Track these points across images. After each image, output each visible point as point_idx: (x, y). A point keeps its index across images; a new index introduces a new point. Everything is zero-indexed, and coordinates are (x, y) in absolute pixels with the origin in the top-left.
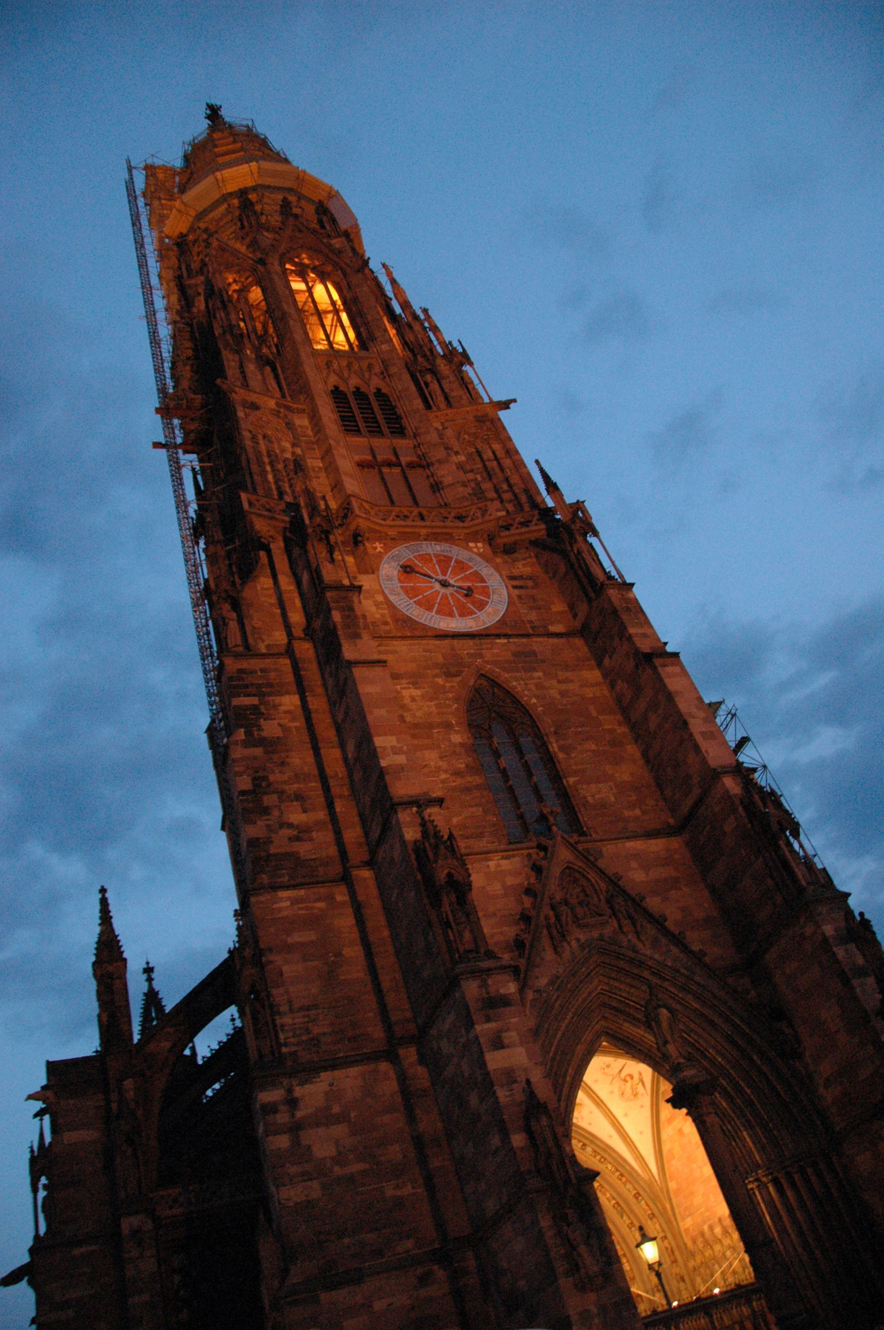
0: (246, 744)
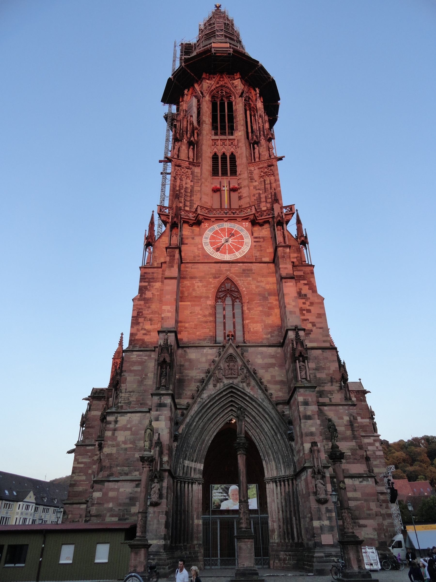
0: (139, 300)
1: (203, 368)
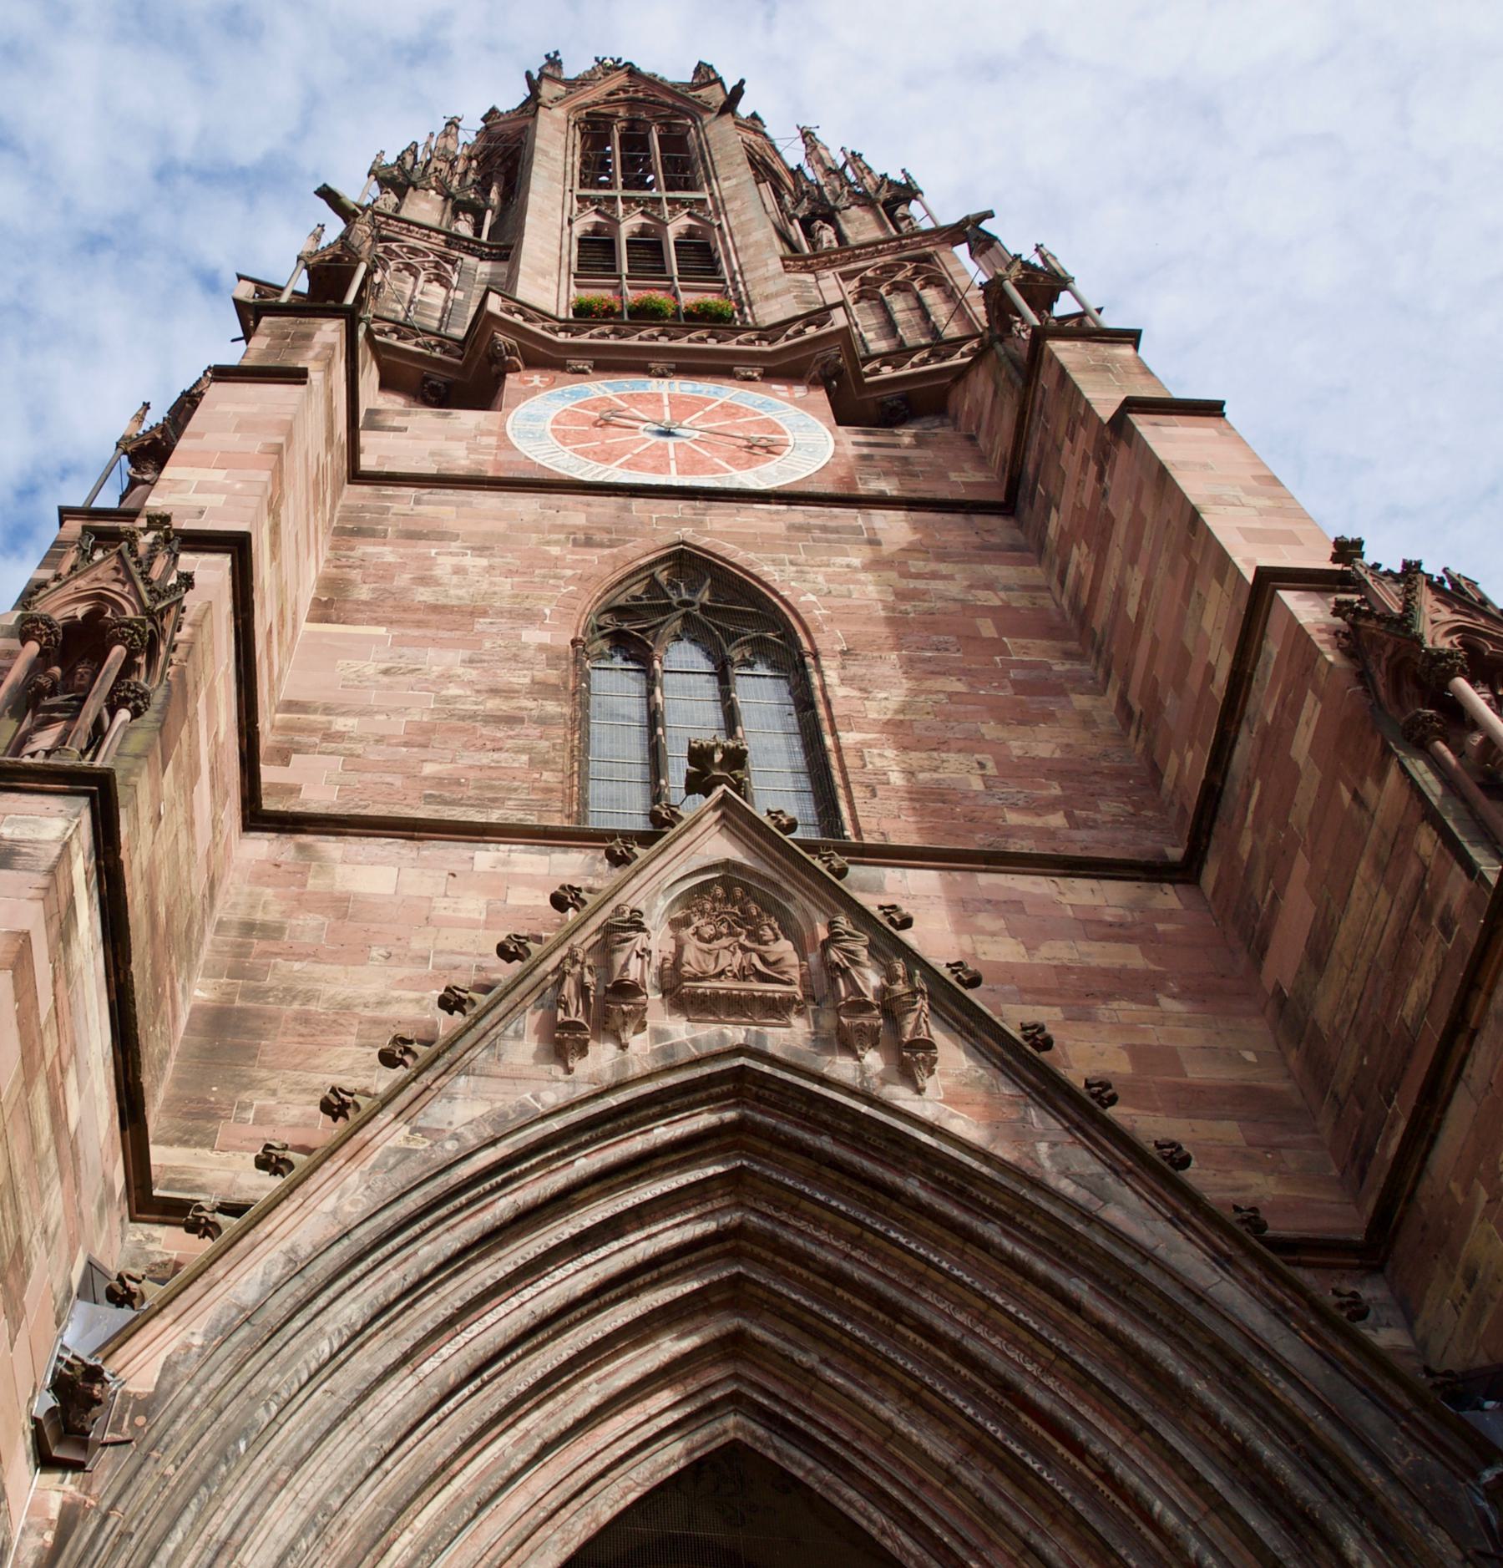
1: (457, 959)
